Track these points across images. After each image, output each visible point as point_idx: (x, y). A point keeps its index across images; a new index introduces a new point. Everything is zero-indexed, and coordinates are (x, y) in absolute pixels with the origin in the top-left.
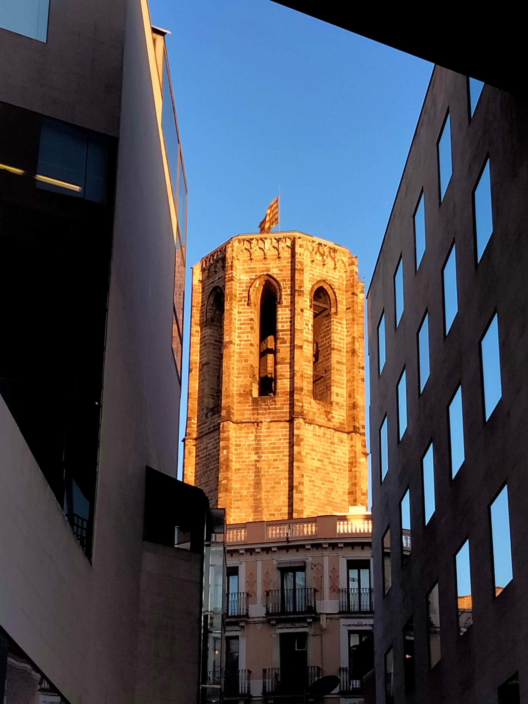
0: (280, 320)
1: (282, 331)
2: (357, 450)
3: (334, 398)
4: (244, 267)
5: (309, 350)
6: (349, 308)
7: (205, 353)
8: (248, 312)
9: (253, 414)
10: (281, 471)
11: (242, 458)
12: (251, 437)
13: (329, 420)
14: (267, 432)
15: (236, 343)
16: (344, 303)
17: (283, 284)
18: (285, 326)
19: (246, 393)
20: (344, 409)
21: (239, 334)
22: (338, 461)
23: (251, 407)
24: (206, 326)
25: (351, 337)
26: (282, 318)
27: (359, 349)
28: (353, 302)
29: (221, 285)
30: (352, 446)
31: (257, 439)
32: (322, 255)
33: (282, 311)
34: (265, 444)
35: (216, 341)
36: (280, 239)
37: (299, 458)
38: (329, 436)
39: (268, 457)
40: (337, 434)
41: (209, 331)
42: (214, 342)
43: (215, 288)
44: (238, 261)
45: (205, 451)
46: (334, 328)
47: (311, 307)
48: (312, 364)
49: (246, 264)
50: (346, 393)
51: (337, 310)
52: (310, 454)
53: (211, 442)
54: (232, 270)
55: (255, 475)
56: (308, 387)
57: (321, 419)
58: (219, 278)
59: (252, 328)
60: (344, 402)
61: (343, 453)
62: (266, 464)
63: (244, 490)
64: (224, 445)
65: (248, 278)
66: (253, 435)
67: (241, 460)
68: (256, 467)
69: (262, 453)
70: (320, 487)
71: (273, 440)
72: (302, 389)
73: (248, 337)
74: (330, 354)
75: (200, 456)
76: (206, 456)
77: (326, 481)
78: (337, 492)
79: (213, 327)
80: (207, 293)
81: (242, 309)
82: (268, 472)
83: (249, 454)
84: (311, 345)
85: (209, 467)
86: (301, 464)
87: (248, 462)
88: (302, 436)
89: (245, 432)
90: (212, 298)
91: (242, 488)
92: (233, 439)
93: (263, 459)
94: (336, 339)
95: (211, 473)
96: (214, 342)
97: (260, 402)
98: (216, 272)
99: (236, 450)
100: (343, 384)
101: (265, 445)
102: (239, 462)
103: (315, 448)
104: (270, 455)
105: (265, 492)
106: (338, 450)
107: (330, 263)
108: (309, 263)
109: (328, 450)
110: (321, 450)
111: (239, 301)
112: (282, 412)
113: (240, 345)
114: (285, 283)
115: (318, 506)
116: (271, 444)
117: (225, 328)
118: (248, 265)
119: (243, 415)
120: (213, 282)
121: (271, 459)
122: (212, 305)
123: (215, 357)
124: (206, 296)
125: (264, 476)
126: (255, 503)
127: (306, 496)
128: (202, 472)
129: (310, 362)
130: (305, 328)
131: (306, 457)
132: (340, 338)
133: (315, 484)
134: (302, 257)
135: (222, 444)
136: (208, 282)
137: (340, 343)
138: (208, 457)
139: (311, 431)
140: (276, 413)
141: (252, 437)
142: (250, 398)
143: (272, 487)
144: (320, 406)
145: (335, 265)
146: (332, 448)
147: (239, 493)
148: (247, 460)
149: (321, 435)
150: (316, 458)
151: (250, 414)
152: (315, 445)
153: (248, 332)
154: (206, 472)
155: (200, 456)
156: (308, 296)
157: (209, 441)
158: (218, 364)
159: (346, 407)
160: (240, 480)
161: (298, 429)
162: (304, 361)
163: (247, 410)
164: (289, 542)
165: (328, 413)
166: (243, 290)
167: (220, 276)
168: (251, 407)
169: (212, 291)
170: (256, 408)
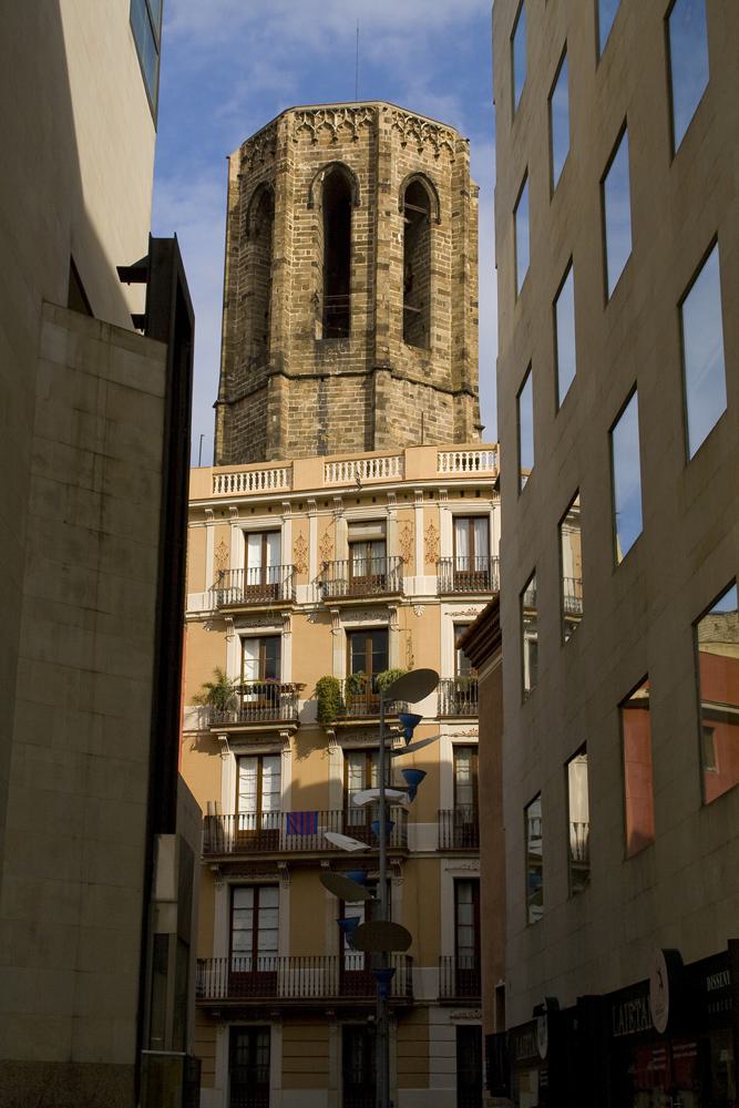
0: (356, 228)
1: (359, 243)
2: (467, 417)
3: (435, 343)
5: (397, 272)
6: (456, 214)
8: (309, 218)
9: (316, 364)
10: (357, 445)
13: (427, 374)
14: (336, 390)
16: (450, 206)
19: (304, 335)
22: (440, 433)
23: (313, 355)
24: (248, 240)
26: (359, 226)
27: (471, 277)
28: (463, 204)
30: (460, 412)
31: (322, 400)
32: (417, 136)
34: (334, 407)
36: (356, 110)
38: (426, 397)
39: (338, 425)
40: (438, 394)
41: (252, 247)
43: (261, 185)
47: (400, 211)
54: (285, 155)
57: (416, 374)
59: (314, 240)
68: (319, 438)
69: (329, 420)
71: (345, 400)
72: (387, 328)
73: (308, 252)
74: (429, 279)
83: (311, 421)
84: (401, 266)
85: (252, 441)
86: (386, 435)
90: (257, 199)
92: (287, 400)
93: (330, 427)
97: (326, 347)
98: (262, 161)
99: (291, 416)
100: (446, 322)
102: (295, 433)
108: (399, 147)
111: (296, 201)
113: (295, 265)
116: (343, 406)
117: (276, 239)
118: (309, 148)
119: (301, 365)
122: (258, 210)
123: (261, 285)
132: (443, 257)
135: (270, 407)
137: (443, 263)
140: (349, 362)
142: (312, 342)
144: (412, 354)
145: (437, 151)
149: (415, 394)
150: (407, 428)
151: (311, 365)
153: (310, 246)
156: (397, 195)
161: (382, 384)
163: (307, 358)
164: (361, 486)
165: (425, 363)
168: (313, 355)
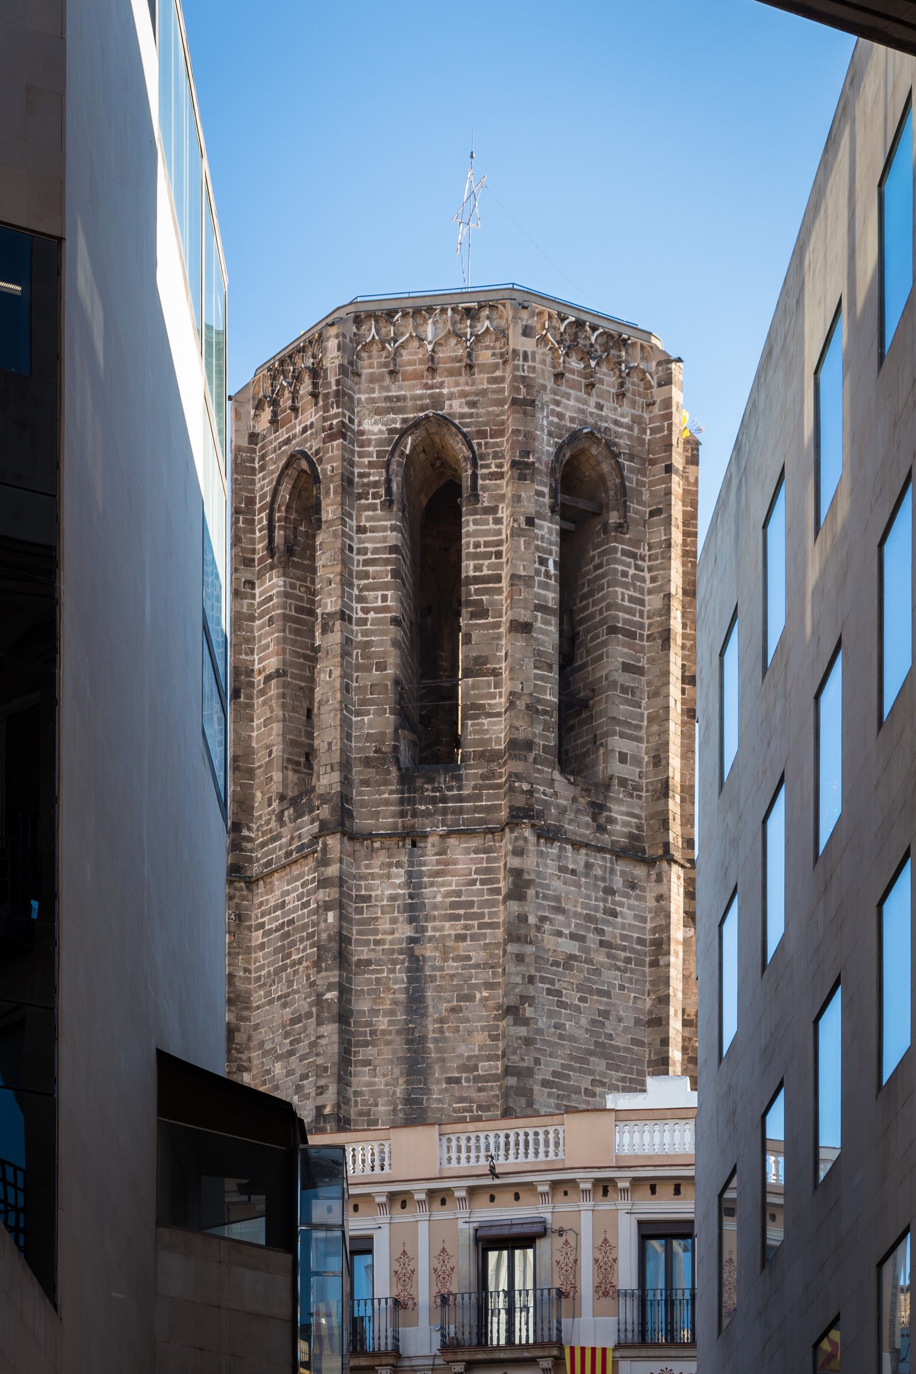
7: (272, 645)
8: (384, 529)
10: (477, 966)
11: (376, 932)
12: (397, 876)
13: (601, 829)
14: (438, 863)
18: (485, 568)
20: (640, 797)
21: (361, 590)
29: (311, 448)
31: (414, 881)
33: (475, 522)
35: (299, 610)
37: (523, 932)
38: (599, 872)
40: (619, 867)
42: (293, 613)
45: (279, 913)
47: (553, 511)
48: (554, 675)
50: (646, 754)
52: (551, 921)
53: (295, 889)
55: (408, 977)
56: (547, 738)
60: (640, 777)
61: (636, 917)
62: (436, 948)
64: (327, 899)
65: (384, 428)
66: (401, 871)
67: (372, 938)
70: (577, 1009)
75: (267, 927)
76: (282, 925)
77: (591, 992)
78: (620, 1020)
79: (292, 571)
81: (369, 519)
82: (442, 969)
85: (289, 955)
87: (391, 943)
88: (529, 873)
89: (382, 863)
91: (374, 1012)
94: (623, 600)
95: (296, 972)
96: (293, 613)
97: (419, 782)
100: (639, 728)
101: (435, 897)
104: (447, 924)
106: (625, 910)
109: (596, 909)
110: (579, 910)
111: (360, 496)
112: (476, 809)
113: (364, 622)
121: (450, 935)
123: (297, 654)
124: (271, 482)
125: (433, 979)
126: (409, 1050)
127: (540, 1031)
128: (272, 969)
129: (550, 668)
130: (538, 573)
131: (538, 928)
132: (632, 599)
133: (564, 999)
138: (286, 929)
139: (552, 860)
140: (460, 811)
141: (399, 876)
143: (453, 1010)
146: (609, 905)
147: (369, 1024)
148: (389, 937)
149: (580, 868)
152: (563, 895)
154: (284, 968)
155: (267, 927)
157: (289, 887)
158: (308, 674)
159: (647, 791)
160: (370, 992)
162: (535, 667)
163: (387, 803)
165: (597, 809)
166: (371, 465)
170: (409, 798)
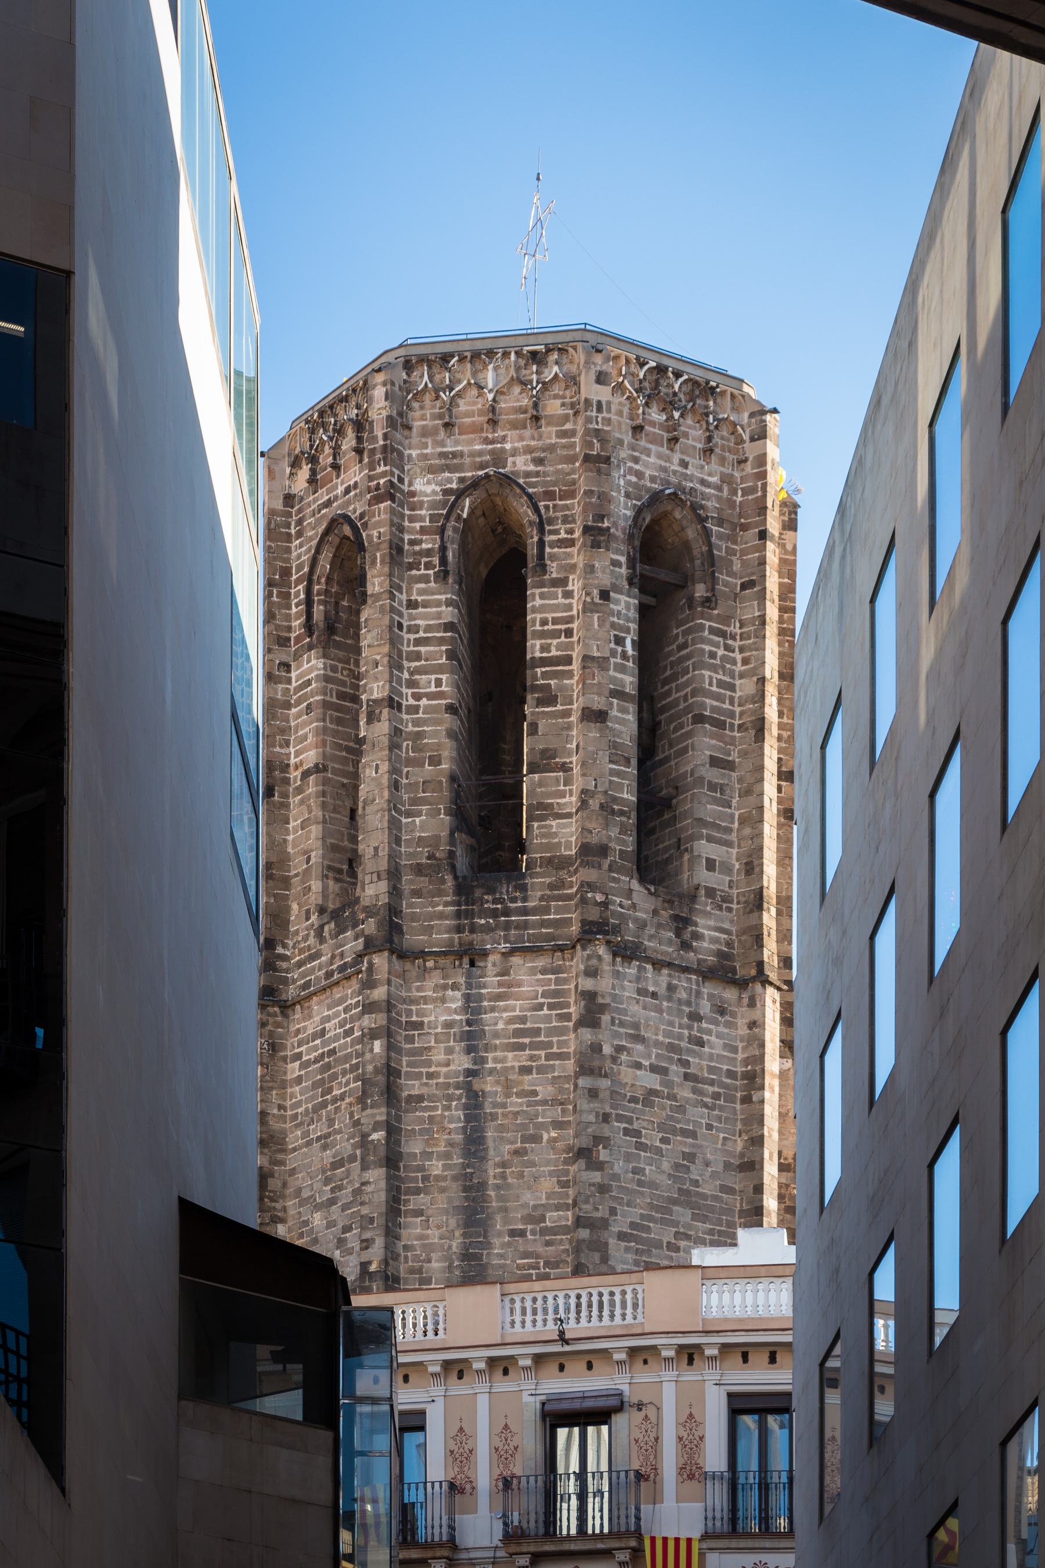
4: (425, 451)
7: (310, 736)
8: (438, 603)
10: (544, 1102)
11: (429, 1063)
12: (453, 1000)
13: (686, 946)
14: (500, 984)
15: (404, 703)
17: (547, 507)
18: (553, 649)
20: (730, 910)
21: (411, 674)
25: (755, 679)
29: (355, 511)
31: (472, 1006)
33: (542, 596)
35: (341, 696)
37: (596, 1063)
38: (684, 995)
40: (707, 989)
42: (334, 700)
44: (406, 432)
45: (318, 1042)
46: (703, 650)
47: (631, 583)
48: (632, 770)
49: (429, 441)
50: (737, 860)
51: (713, 589)
52: (628, 1051)
53: (337, 1015)
55: (465, 1115)
56: (624, 843)
58: (347, 491)
60: (730, 887)
61: (726, 1046)
62: (498, 1082)
63: (434, 1162)
64: (373, 1025)
65: (438, 489)
66: (458, 994)
67: (424, 1070)
70: (659, 1151)
75: (304, 1058)
76: (322, 1056)
77: (674, 1132)
78: (707, 1164)
79: (333, 651)
80: (311, 539)
81: (421, 592)
82: (504, 1106)
85: (330, 1090)
87: (446, 1076)
89: (436, 985)
91: (427, 1155)
94: (710, 684)
95: (337, 1109)
96: (334, 700)
97: (478, 893)
100: (729, 830)
101: (496, 1024)
103: (643, 1033)
104: (510, 1055)
105: (497, 1165)
106: (713, 1039)
107: (693, 434)
108: (627, 438)
109: (680, 1037)
110: (661, 1038)
111: (411, 567)
112: (543, 924)
113: (415, 709)
114: (551, 504)
115: (652, 1207)
120: (328, 504)
121: (513, 1067)
123: (339, 747)
124: (309, 550)
125: (494, 1117)
126: (467, 1198)
127: (616, 1177)
128: (310, 1106)
129: (627, 762)
130: (613, 653)
131: (614, 1059)
132: (721, 684)
133: (643, 1140)
134: (605, 414)
136: (315, 500)
138: (327, 1060)
139: (630, 982)
140: (525, 925)
141: (455, 1000)
143: (517, 1152)
145: (709, 439)
146: (695, 1033)
147: (421, 1168)
148: (444, 1070)
149: (662, 990)
152: (643, 1021)
154: (324, 1105)
155: (304, 1058)
157: (330, 1012)
158: (351, 769)
159: (738, 903)
160: (422, 1132)
162: (611, 762)
163: (441, 916)
165: (682, 923)
166: (423, 530)
167: (352, 483)
169: (327, 532)
170: (467, 910)
